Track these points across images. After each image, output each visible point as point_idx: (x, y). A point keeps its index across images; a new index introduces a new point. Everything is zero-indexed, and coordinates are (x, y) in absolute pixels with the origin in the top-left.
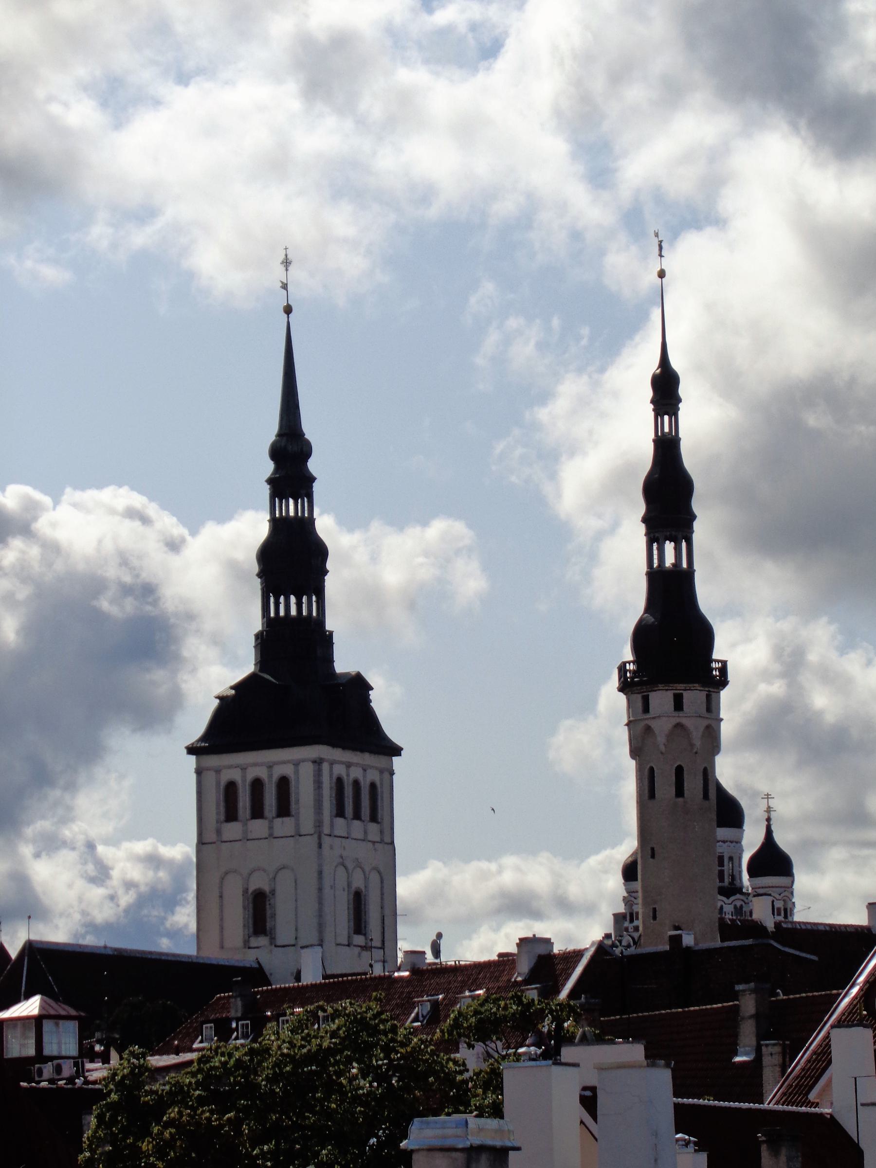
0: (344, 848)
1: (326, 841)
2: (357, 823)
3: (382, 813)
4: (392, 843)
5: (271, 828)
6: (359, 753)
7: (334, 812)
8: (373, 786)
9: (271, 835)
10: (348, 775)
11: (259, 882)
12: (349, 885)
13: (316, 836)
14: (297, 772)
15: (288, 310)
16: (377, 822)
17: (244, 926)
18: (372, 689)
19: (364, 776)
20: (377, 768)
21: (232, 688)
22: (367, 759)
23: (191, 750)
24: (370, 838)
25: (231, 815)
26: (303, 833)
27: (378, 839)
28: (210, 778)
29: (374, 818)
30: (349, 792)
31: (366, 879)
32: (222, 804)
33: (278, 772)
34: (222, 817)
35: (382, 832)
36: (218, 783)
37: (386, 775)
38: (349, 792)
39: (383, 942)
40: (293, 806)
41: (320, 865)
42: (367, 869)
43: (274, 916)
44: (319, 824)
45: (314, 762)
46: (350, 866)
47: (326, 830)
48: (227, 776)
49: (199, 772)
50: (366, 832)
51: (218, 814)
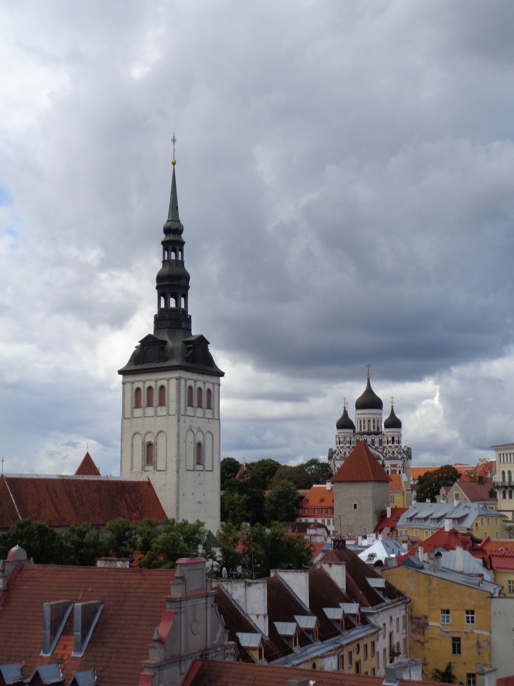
0: (192, 422)
1: (182, 418)
2: (199, 410)
3: (214, 404)
4: (219, 419)
5: (156, 411)
6: (201, 375)
7: (187, 404)
8: (209, 391)
10: (195, 385)
11: (150, 438)
12: (195, 439)
13: (176, 415)
14: (168, 384)
15: (174, 164)
16: (211, 409)
17: (142, 459)
18: (209, 343)
19: (204, 386)
20: (211, 383)
21: (139, 342)
22: (206, 378)
23: (120, 372)
24: (207, 416)
25: (137, 405)
26: (170, 414)
27: (211, 417)
28: (128, 386)
29: (209, 407)
30: (195, 393)
32: (134, 399)
33: (160, 383)
34: (134, 406)
35: (213, 414)
36: (132, 388)
37: (216, 386)
38: (195, 393)
39: (213, 468)
40: (166, 401)
41: (179, 430)
43: (156, 455)
44: (178, 410)
45: (177, 379)
46: (195, 431)
47: (182, 413)
49: (124, 384)
50: (204, 414)
51: (132, 404)
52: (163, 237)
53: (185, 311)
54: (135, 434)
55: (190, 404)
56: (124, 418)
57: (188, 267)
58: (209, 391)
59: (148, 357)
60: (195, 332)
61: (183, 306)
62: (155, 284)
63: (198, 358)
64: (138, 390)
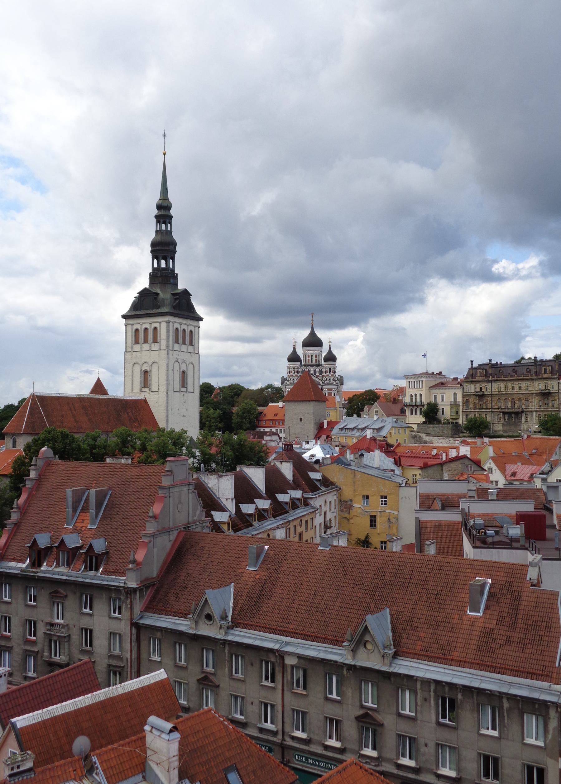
1: (171, 352)
4: (198, 353)
9: (150, 349)
12: (180, 369)
14: (160, 326)
15: (164, 154)
19: (187, 328)
22: (189, 322)
23: (123, 317)
25: (136, 342)
28: (130, 327)
29: (191, 344)
33: (154, 325)
35: (194, 349)
36: (132, 329)
37: (197, 328)
39: (194, 390)
40: (158, 338)
42: (188, 363)
43: (151, 380)
44: (168, 346)
48: (136, 327)
49: (126, 325)
50: (187, 349)
52: (156, 212)
53: (173, 270)
55: (177, 342)
56: (126, 351)
57: (175, 236)
58: (191, 331)
60: (181, 286)
61: (171, 266)
62: (150, 249)
63: (183, 306)
64: (137, 330)
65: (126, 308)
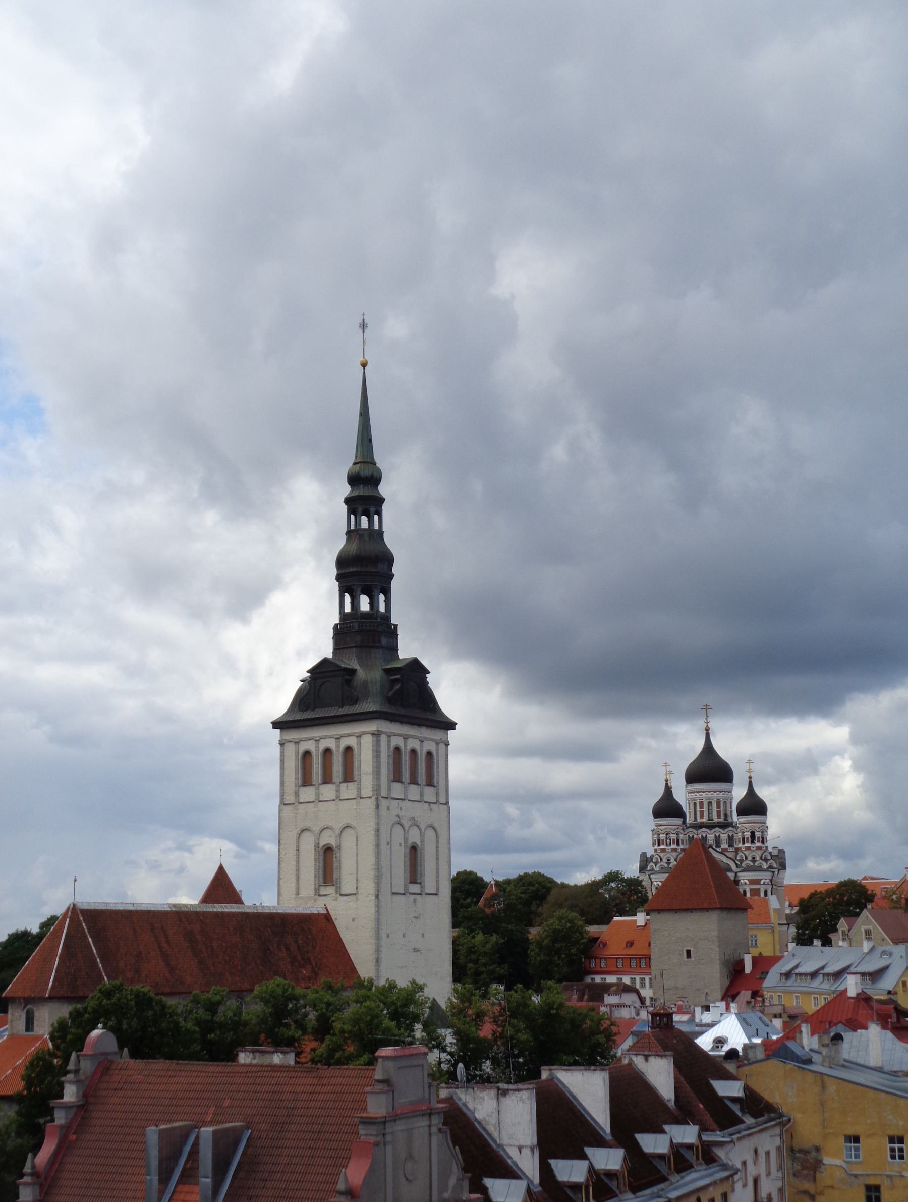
0: (401, 809)
1: (384, 803)
2: (413, 787)
3: (439, 778)
4: (447, 803)
5: (338, 791)
6: (416, 727)
7: (392, 777)
8: (429, 754)
9: (338, 797)
10: (405, 746)
11: (328, 839)
12: (406, 839)
13: (374, 798)
14: (359, 743)
15: (364, 365)
16: (434, 786)
17: (315, 876)
19: (421, 746)
20: (432, 740)
21: (308, 672)
22: (425, 732)
23: (277, 724)
24: (426, 799)
25: (306, 781)
26: (364, 795)
27: (434, 800)
28: (290, 748)
29: (430, 783)
30: (406, 759)
31: (422, 835)
32: (300, 770)
34: (300, 783)
35: (437, 794)
36: (297, 752)
37: (442, 746)
38: (406, 759)
40: (356, 772)
41: (378, 824)
42: (423, 827)
43: (340, 868)
44: (377, 789)
45: (373, 734)
46: (406, 824)
47: (384, 793)
48: (304, 747)
49: (282, 744)
50: (422, 795)
51: (296, 778)
53: (387, 617)
54: (303, 830)
56: (283, 803)
58: (429, 754)
59: (324, 697)
60: (406, 650)
61: (382, 608)
62: (334, 572)
63: (410, 698)
64: (307, 754)
65: (281, 702)
